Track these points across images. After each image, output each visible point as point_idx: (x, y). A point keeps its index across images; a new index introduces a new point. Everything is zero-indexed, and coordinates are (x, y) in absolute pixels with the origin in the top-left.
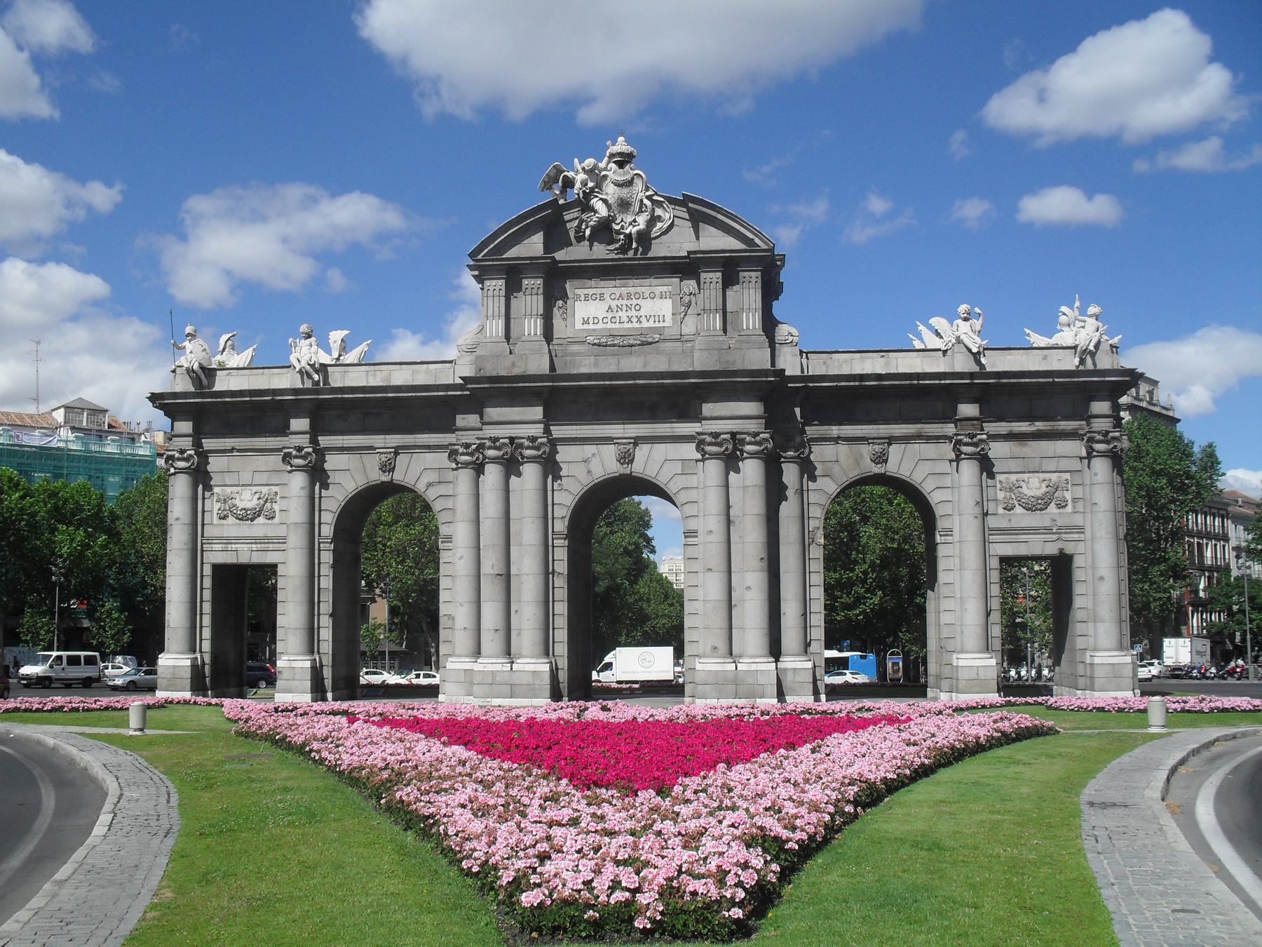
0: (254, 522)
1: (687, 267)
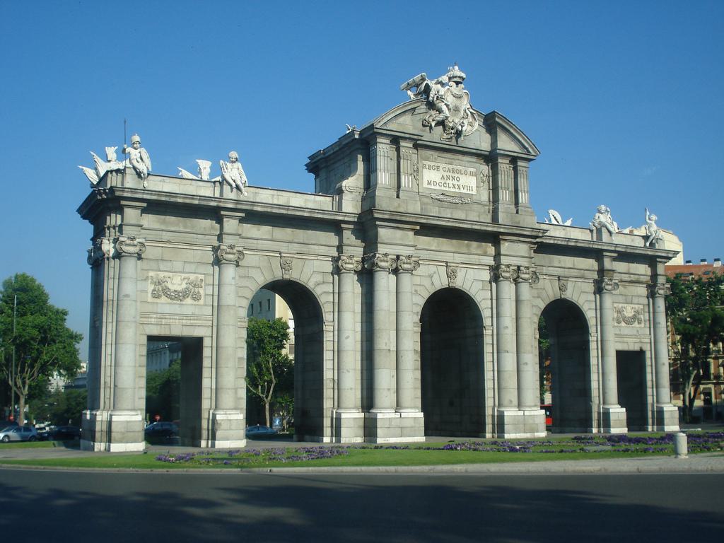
0: (184, 303)
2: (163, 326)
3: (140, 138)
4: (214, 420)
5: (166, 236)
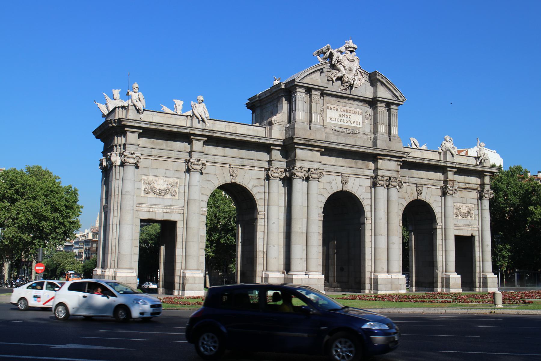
0: (165, 197)
2: (151, 213)
3: (139, 85)
4: (184, 278)
5: (154, 152)
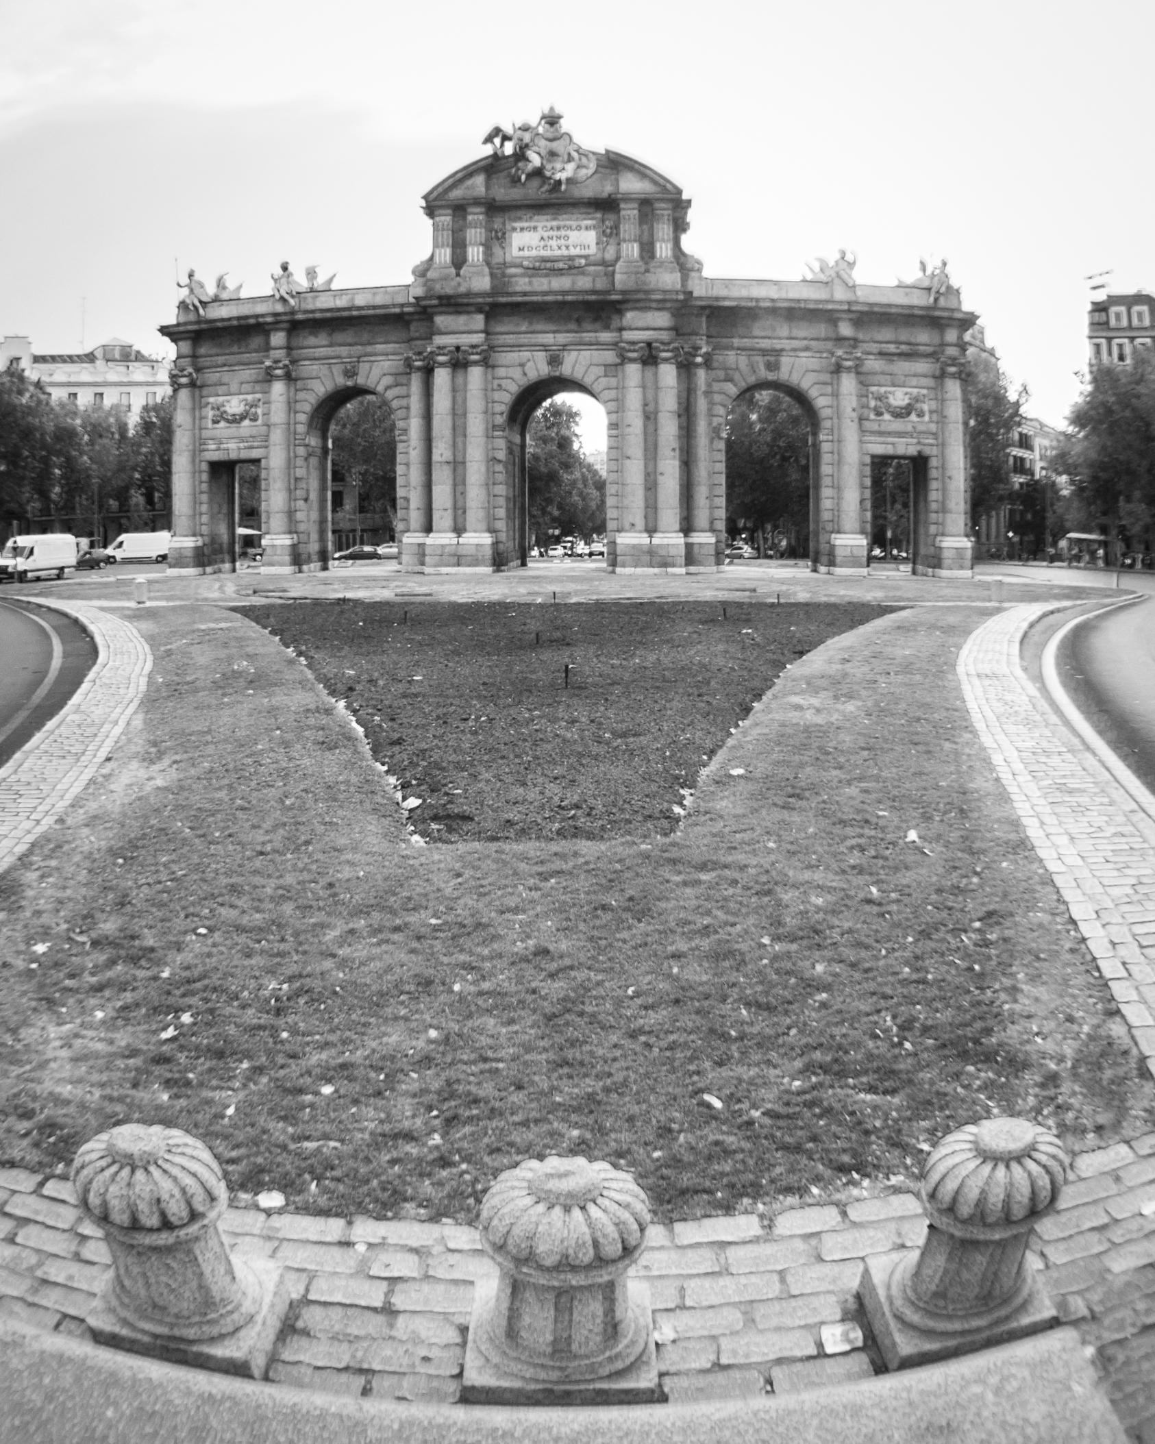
1: (606, 206)
5: (221, 360)
